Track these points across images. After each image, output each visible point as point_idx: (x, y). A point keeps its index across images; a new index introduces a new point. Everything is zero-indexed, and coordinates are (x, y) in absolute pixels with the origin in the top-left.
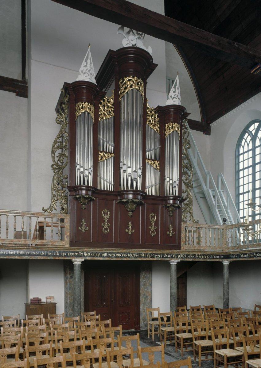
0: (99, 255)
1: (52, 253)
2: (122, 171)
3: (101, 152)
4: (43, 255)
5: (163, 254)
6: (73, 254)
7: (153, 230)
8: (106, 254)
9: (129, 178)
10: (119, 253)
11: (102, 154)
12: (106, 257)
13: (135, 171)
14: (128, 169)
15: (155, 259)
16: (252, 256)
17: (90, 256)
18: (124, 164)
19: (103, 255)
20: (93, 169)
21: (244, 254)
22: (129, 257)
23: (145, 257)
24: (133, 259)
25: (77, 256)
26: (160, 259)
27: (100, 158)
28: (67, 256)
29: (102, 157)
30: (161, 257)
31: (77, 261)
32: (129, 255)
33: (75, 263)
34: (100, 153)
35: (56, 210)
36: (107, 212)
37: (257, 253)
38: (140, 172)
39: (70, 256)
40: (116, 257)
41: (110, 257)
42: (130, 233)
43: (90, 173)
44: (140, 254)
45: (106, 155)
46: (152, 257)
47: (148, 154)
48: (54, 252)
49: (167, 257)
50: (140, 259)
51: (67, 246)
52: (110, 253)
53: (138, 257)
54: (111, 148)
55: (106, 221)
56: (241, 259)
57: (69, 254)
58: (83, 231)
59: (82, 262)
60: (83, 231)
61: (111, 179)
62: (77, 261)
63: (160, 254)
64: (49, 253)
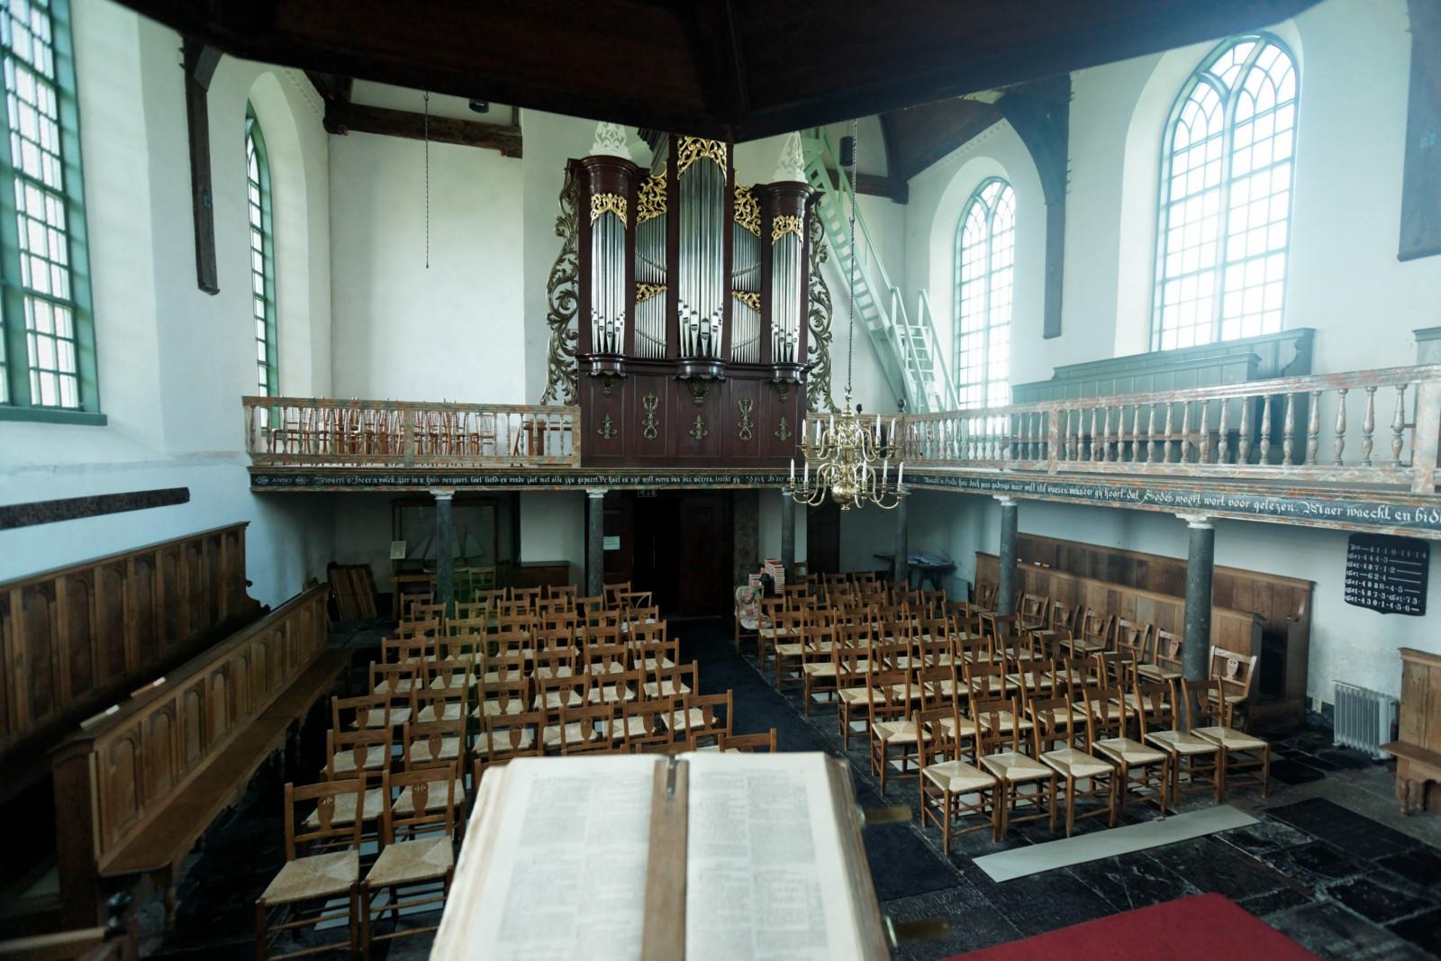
0: (637, 480)
1: (548, 480)
2: (681, 319)
3: (641, 284)
4: (532, 484)
5: (766, 477)
6: (587, 480)
7: (745, 428)
8: (650, 479)
9: (695, 334)
10: (676, 476)
11: (643, 288)
12: (651, 483)
13: (705, 320)
14: (693, 316)
15: (750, 486)
16: (942, 482)
17: (621, 483)
18: (685, 307)
19: (644, 480)
20: (626, 319)
21: (931, 477)
22: (697, 483)
23: (729, 483)
24: (704, 486)
25: (594, 484)
26: (759, 486)
27: (639, 296)
28: (576, 483)
29: (643, 294)
30: (761, 482)
31: (597, 493)
32: (696, 480)
33: (591, 496)
34: (638, 285)
35: (555, 399)
36: (654, 399)
37: (950, 478)
38: (715, 321)
39: (582, 484)
40: (671, 483)
41: (658, 483)
42: (699, 437)
43: (618, 329)
44: (719, 476)
45: (652, 289)
46: (744, 481)
47: (736, 280)
48: (552, 477)
49: (775, 482)
50: (719, 487)
51: (576, 466)
52: (659, 476)
53: (715, 483)
54: (661, 275)
55: (651, 416)
56: (925, 487)
57: (579, 480)
58: (607, 437)
59: (605, 495)
60: (607, 437)
61: (662, 337)
62: (597, 493)
63: (760, 476)
64: (542, 480)
